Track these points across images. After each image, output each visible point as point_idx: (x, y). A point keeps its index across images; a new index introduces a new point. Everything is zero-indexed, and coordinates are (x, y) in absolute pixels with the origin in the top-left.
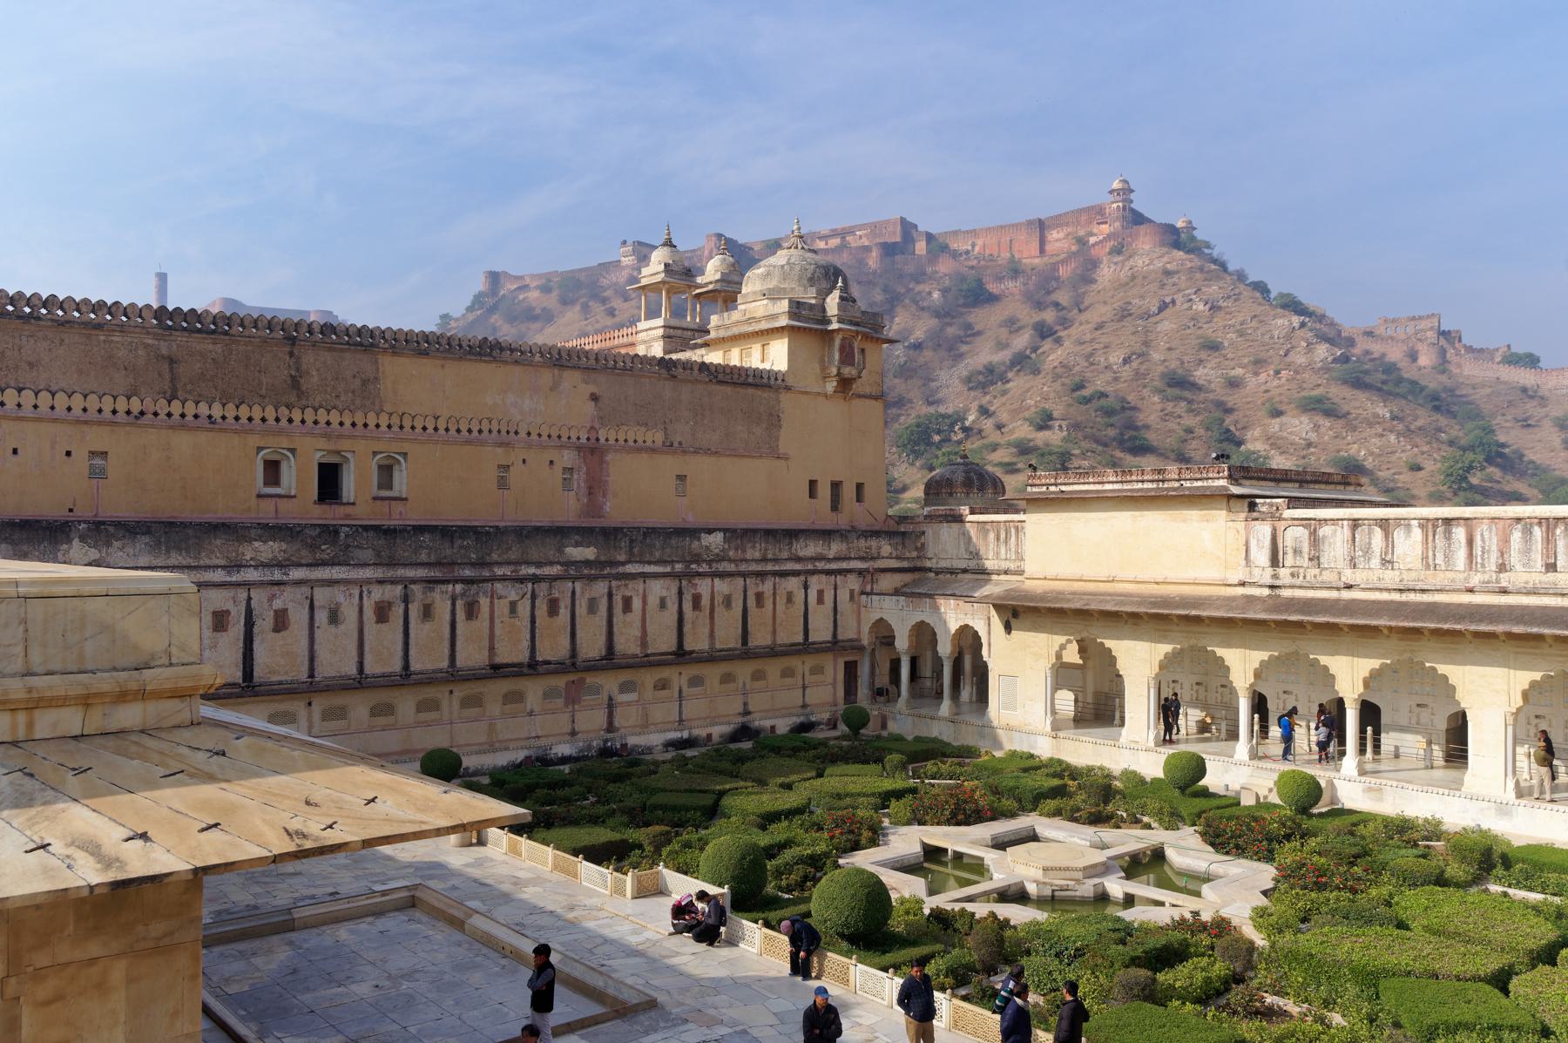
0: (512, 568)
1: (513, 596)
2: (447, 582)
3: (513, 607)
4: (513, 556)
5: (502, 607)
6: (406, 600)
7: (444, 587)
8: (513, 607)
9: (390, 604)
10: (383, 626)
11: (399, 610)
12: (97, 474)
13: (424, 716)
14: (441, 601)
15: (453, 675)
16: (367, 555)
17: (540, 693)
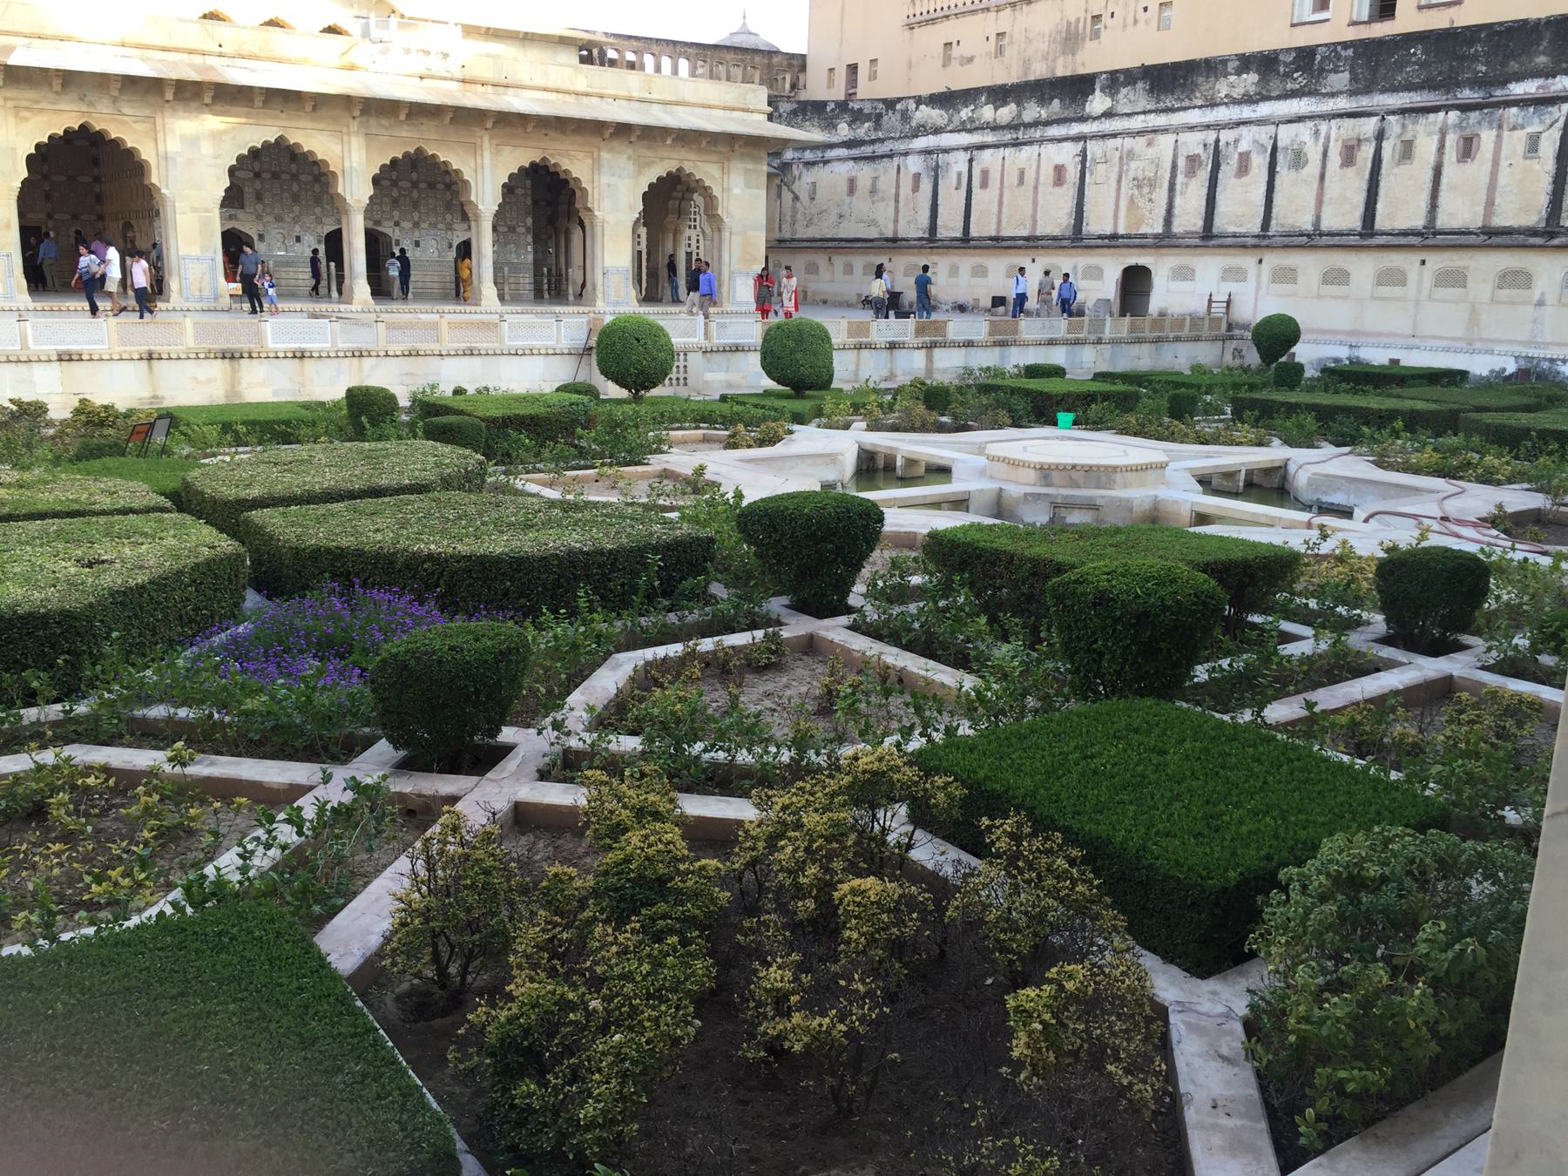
0: (1540, 82)
1: (1535, 128)
2: (1435, 109)
3: (1533, 144)
4: (1542, 60)
5: (1515, 141)
6: (1380, 136)
7: (1432, 116)
8: (1533, 144)
9: (1359, 140)
10: (1350, 171)
11: (1367, 151)
12: (1163, 25)
13: (1385, 291)
14: (1425, 135)
15: (1429, 238)
16: (1341, 80)
17: (1559, 277)
